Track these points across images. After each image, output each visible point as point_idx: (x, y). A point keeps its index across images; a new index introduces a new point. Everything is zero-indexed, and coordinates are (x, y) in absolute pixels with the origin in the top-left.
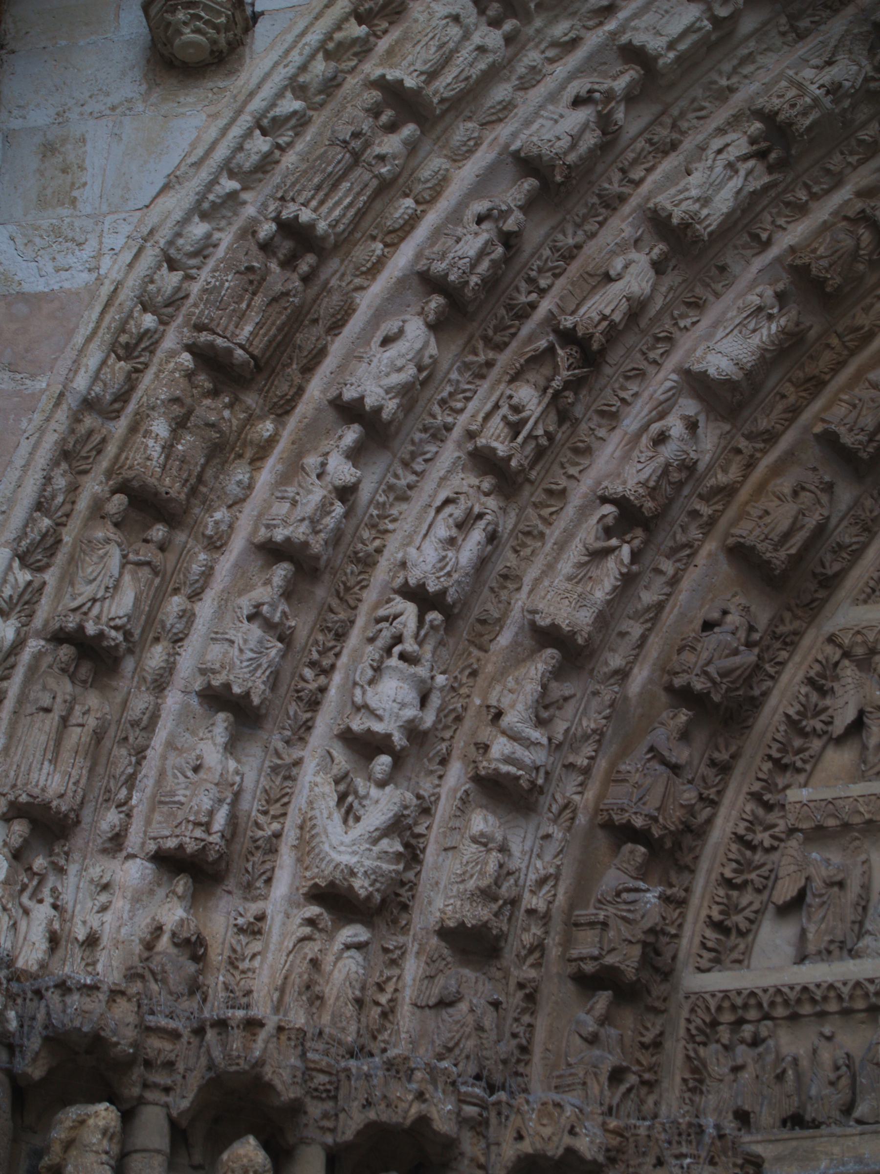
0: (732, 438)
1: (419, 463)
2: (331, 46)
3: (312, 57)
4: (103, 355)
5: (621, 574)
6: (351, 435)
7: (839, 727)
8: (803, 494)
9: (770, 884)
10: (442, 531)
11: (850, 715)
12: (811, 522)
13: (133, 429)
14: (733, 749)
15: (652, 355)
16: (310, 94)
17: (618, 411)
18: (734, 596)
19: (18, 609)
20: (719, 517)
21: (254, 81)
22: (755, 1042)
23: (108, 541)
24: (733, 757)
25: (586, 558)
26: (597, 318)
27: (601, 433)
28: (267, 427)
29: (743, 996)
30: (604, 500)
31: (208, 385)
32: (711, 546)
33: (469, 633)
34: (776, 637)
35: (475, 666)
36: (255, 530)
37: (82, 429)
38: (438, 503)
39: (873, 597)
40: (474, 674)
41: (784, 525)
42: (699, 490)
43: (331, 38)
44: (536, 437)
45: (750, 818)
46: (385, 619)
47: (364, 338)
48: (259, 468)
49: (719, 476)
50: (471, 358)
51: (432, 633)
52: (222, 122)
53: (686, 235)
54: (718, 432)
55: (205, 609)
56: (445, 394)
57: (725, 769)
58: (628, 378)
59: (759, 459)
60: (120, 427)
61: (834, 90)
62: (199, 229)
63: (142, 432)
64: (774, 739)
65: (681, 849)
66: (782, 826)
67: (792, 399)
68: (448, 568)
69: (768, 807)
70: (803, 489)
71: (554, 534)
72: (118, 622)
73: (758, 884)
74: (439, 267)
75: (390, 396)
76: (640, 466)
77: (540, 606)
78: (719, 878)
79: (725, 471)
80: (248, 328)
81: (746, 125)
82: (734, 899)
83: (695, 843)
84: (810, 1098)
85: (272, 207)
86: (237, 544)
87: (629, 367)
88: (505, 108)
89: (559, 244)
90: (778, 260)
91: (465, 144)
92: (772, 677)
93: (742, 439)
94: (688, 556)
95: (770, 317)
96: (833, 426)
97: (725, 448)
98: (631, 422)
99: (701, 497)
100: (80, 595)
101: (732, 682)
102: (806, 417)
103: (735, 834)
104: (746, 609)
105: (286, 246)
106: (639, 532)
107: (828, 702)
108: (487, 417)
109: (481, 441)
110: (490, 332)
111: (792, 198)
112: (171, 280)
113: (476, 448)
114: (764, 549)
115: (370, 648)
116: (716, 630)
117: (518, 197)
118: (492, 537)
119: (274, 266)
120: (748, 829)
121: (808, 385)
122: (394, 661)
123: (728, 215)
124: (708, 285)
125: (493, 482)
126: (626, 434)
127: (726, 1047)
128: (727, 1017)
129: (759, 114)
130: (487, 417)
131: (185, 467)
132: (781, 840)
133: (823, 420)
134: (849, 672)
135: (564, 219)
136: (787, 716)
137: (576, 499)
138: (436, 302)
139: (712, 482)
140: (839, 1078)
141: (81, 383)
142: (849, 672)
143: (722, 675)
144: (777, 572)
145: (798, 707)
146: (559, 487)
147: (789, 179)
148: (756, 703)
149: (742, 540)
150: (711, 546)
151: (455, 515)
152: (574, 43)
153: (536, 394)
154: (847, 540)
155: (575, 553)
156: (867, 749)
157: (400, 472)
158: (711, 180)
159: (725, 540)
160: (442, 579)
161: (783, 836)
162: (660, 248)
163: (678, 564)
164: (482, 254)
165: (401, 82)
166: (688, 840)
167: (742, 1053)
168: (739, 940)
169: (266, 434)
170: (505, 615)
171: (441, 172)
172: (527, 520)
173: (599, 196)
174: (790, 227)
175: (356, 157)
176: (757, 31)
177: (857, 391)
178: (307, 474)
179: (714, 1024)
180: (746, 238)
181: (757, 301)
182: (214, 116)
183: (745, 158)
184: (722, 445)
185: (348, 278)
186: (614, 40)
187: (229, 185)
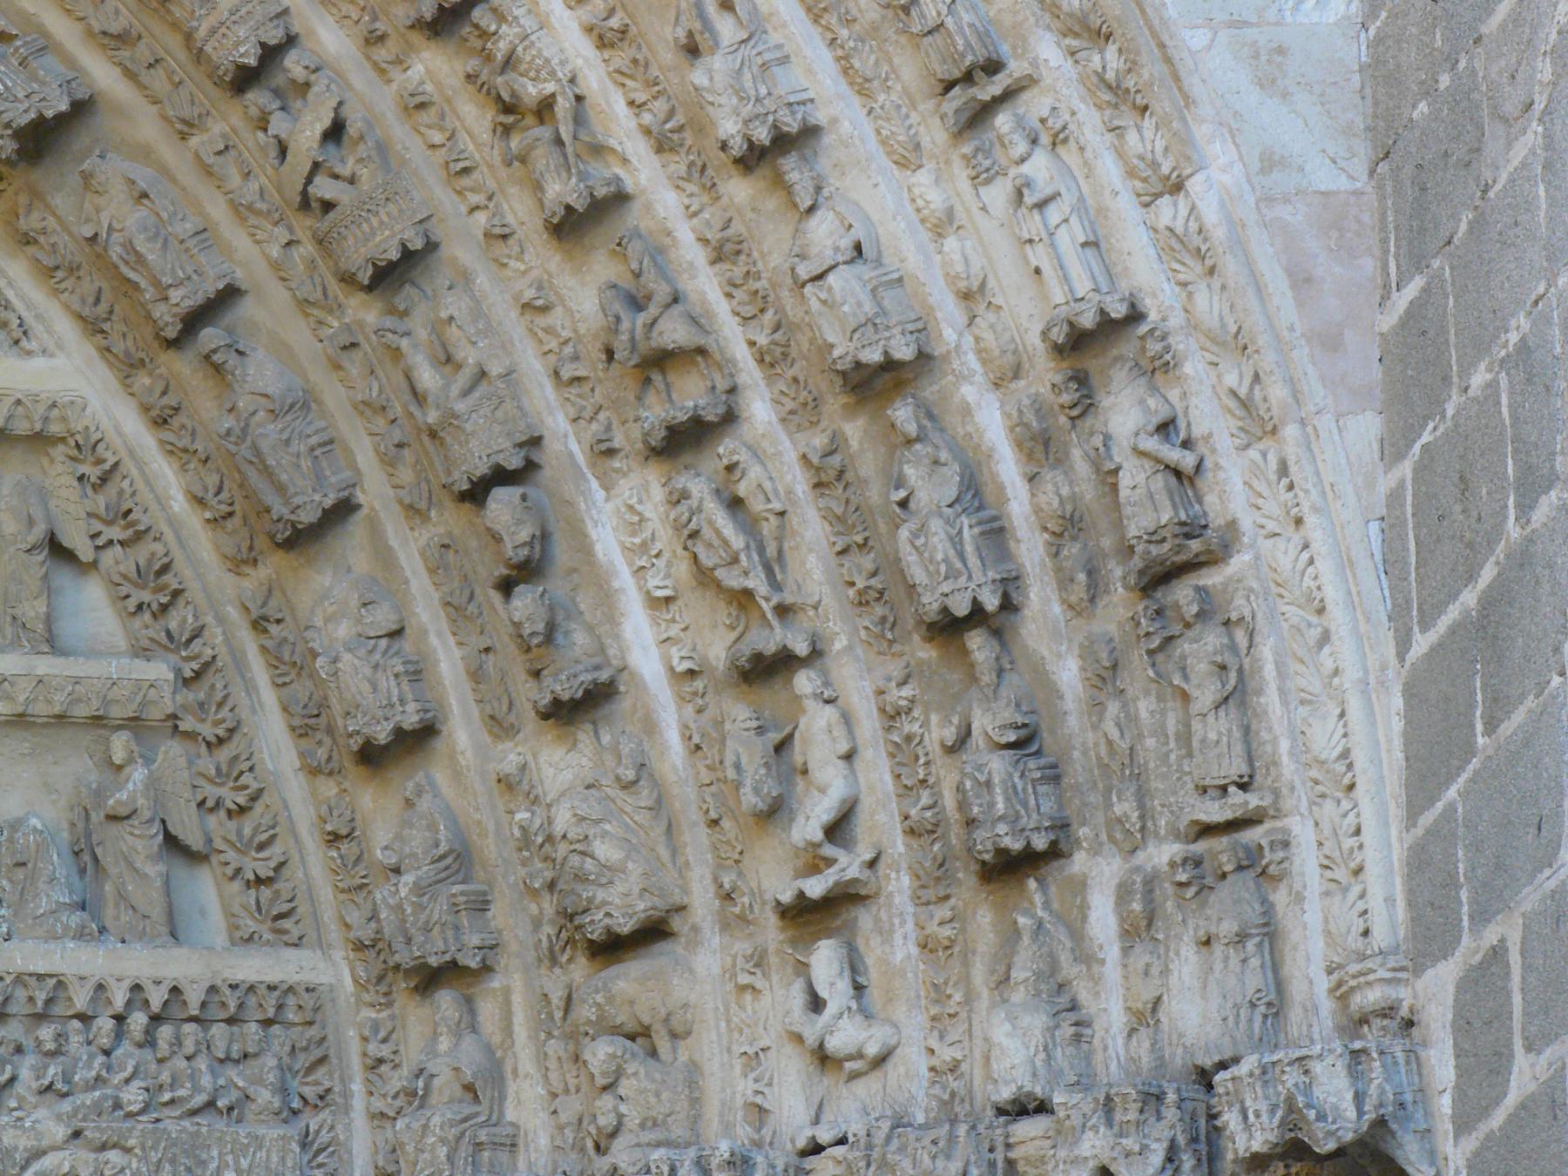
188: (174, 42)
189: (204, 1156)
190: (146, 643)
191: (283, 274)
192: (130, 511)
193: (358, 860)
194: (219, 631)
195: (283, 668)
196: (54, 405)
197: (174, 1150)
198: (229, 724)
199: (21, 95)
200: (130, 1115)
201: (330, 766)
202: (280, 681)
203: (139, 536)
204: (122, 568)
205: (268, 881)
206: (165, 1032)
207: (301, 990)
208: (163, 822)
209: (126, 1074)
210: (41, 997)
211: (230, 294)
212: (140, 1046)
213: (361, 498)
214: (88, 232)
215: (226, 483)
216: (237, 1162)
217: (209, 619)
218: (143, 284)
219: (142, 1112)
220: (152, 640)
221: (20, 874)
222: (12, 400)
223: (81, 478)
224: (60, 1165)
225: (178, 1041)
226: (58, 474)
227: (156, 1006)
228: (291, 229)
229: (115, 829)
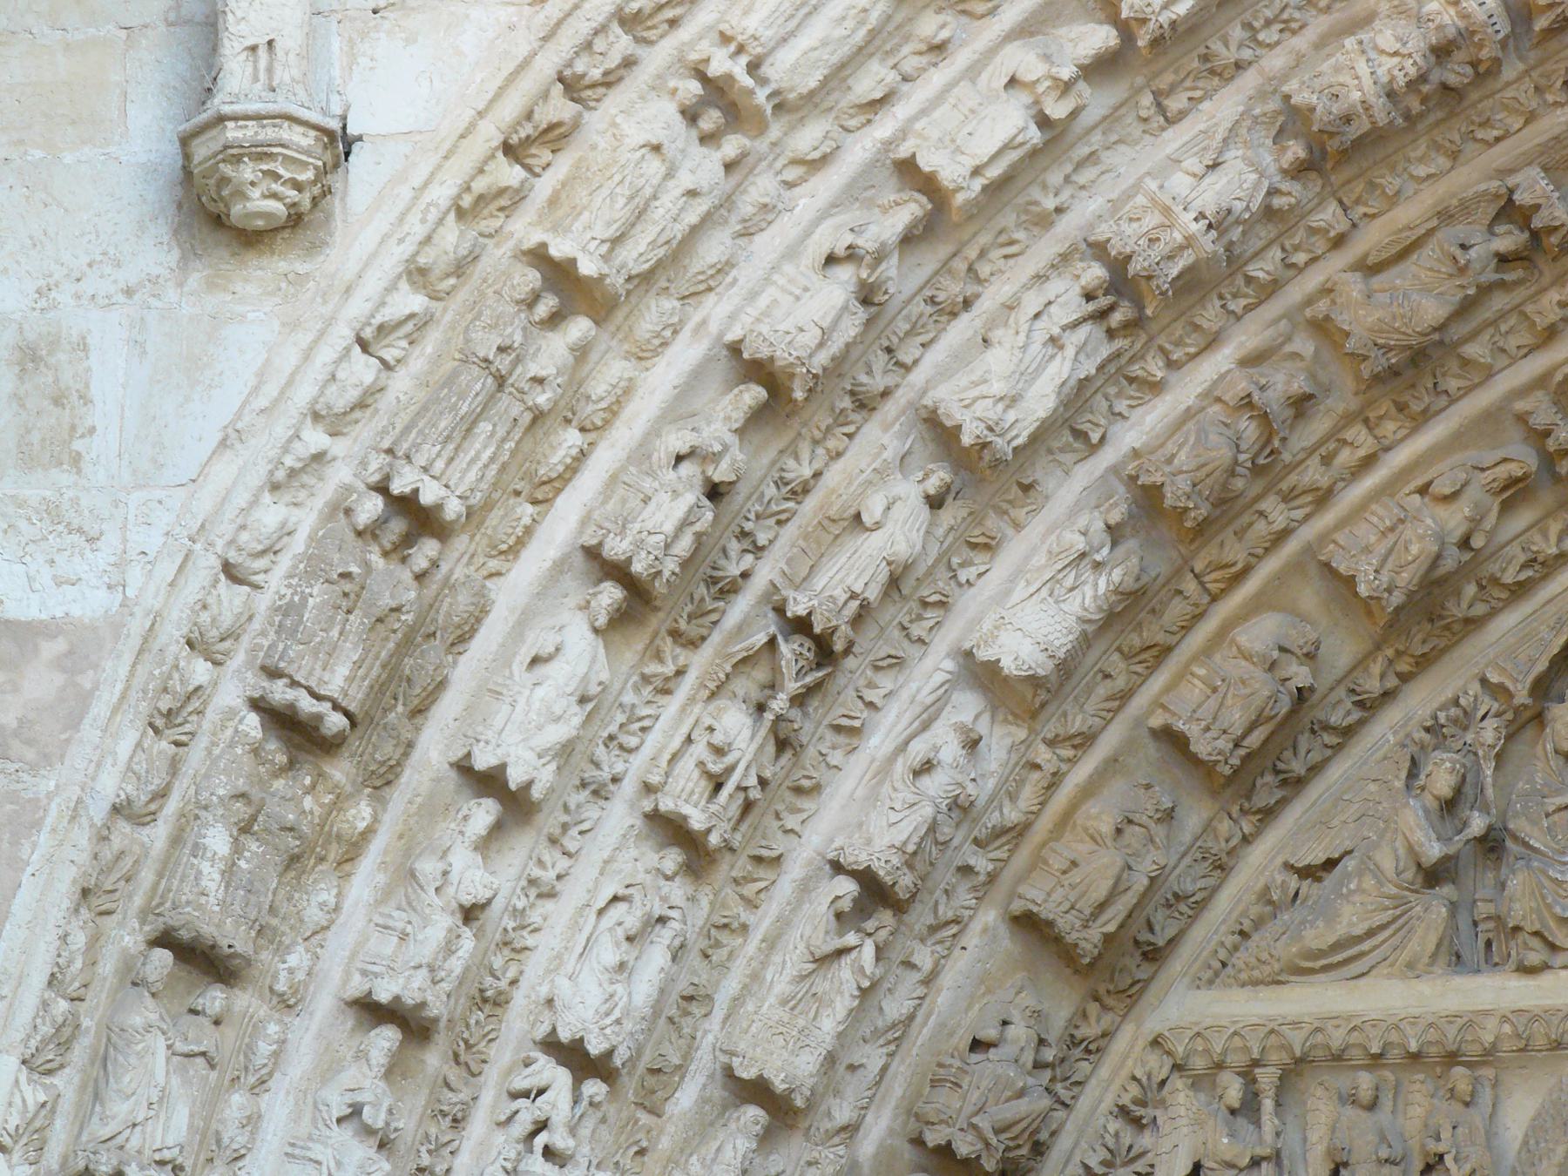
1: (573, 838)
2: (467, 201)
3: (441, 221)
4: (138, 735)
5: (859, 988)
6: (484, 813)
8: (1130, 830)
10: (608, 953)
13: (176, 840)
15: (917, 630)
16: (433, 277)
19: (24, 1140)
21: (352, 267)
23: (148, 1028)
25: (812, 966)
26: (845, 596)
27: (836, 758)
28: (360, 813)
30: (837, 867)
31: (282, 759)
33: (636, 1094)
34: (1074, 1042)
35: (644, 1144)
36: (346, 981)
37: (107, 854)
38: (601, 904)
40: (641, 1152)
41: (1100, 891)
42: (976, 833)
43: (468, 189)
44: (746, 789)
46: (525, 1094)
47: (503, 659)
48: (349, 875)
49: (1006, 811)
50: (652, 668)
51: (591, 1111)
52: (304, 339)
53: (981, 458)
54: (1008, 741)
55: (278, 1107)
56: (613, 728)
58: (877, 668)
60: (157, 835)
61: (1218, 224)
62: (271, 515)
63: (189, 845)
68: (617, 1014)
70: (1130, 822)
71: (762, 922)
72: (167, 1155)
74: (616, 548)
75: (543, 761)
76: (894, 817)
77: (742, 1047)
79: (1013, 797)
80: (343, 670)
81: (1080, 265)
85: (377, 462)
86: (324, 1003)
87: (883, 654)
88: (719, 271)
89: (788, 476)
90: (1114, 470)
91: (658, 335)
93: (1042, 748)
94: (954, 936)
95: (1098, 566)
96: (1180, 724)
97: (1017, 764)
98: (878, 742)
99: (976, 842)
100: (113, 1118)
101: (1012, 1139)
104: (1037, 1014)
105: (397, 526)
107: (1146, 1140)
108: (674, 758)
109: (666, 804)
110: (683, 625)
111: (1140, 373)
112: (232, 598)
113: (656, 810)
115: (500, 1138)
116: (992, 1052)
117: (734, 415)
118: (678, 953)
119: (376, 558)
122: (536, 1163)
123: (1044, 421)
124: (1006, 512)
125: (680, 859)
129: (1099, 250)
130: (674, 758)
131: (253, 899)
134: (1181, 1098)
135: (800, 434)
137: (794, 871)
138: (610, 594)
139: (993, 819)
141: (109, 786)
142: (1181, 1097)
143: (997, 1132)
145: (1103, 1154)
146: (774, 854)
147: (1138, 346)
149: (1035, 909)
150: (989, 916)
151: (628, 925)
152: (825, 160)
153: (749, 721)
154: (1189, 887)
155: (791, 959)
157: (546, 858)
158: (1022, 368)
159: (1009, 904)
160: (608, 1031)
162: (939, 477)
164: (685, 523)
165: (573, 261)
169: (362, 826)
170: (687, 1056)
171: (623, 384)
172: (724, 906)
173: (852, 393)
174: (1135, 415)
175: (501, 381)
176: (1105, 118)
178: (422, 888)
180: (1067, 437)
181: (1080, 544)
182: (292, 325)
183: (1075, 325)
184: (1012, 762)
185: (480, 560)
186: (887, 151)
187: (316, 438)
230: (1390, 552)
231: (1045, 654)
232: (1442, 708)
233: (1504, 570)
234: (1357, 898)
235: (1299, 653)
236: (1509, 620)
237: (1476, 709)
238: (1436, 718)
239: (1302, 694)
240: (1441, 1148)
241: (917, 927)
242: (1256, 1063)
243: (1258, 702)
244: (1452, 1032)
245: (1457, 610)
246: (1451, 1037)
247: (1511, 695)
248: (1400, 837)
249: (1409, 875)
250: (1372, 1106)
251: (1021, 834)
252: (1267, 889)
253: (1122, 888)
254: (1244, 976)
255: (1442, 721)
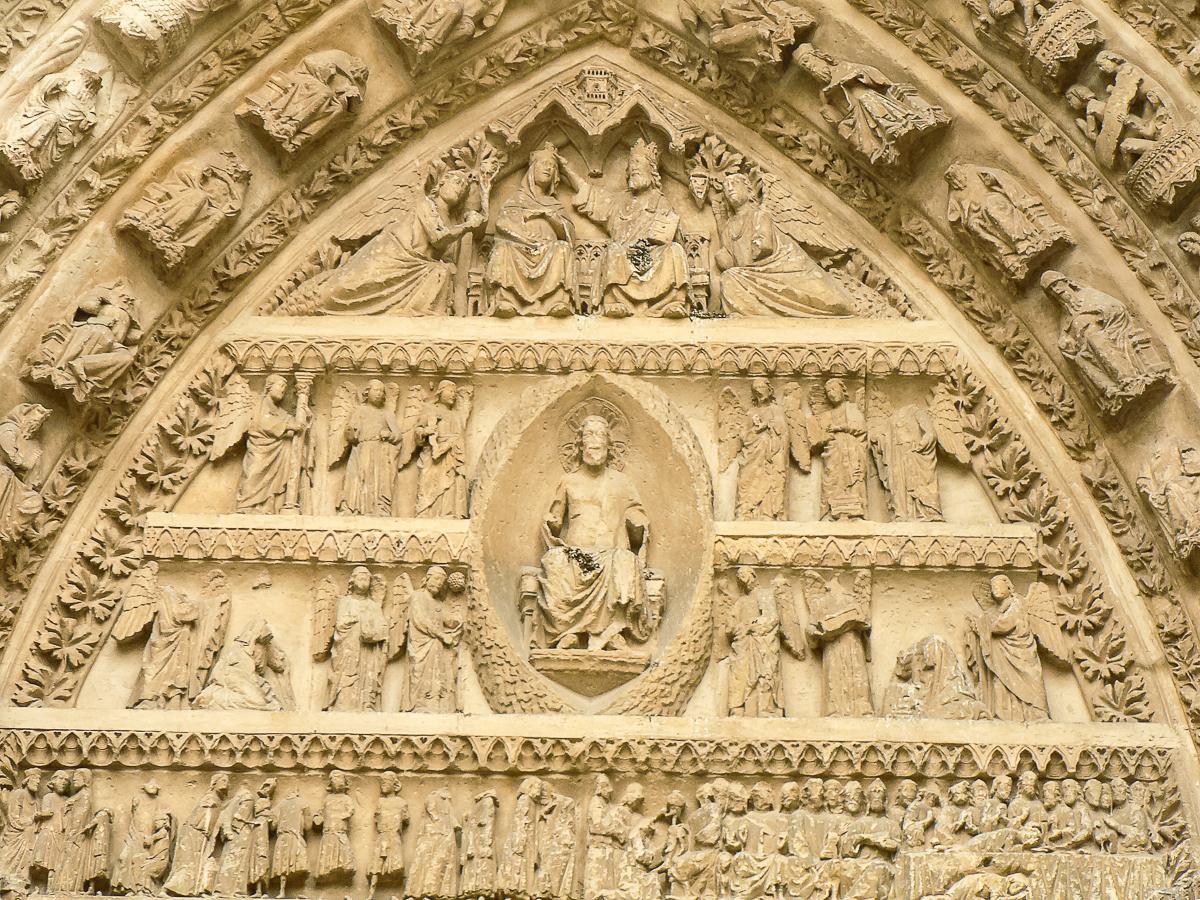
0: (141, 105)
7: (218, 450)
8: (213, 181)
9: (114, 615)
11: (234, 438)
12: (218, 214)
14: (93, 458)
17: (8, 54)
18: (118, 285)
20: (113, 193)
22: (67, 792)
24: (90, 467)
29: (61, 737)
32: (100, 225)
34: (161, 339)
39: (279, 308)
41: (185, 214)
45: (102, 539)
54: (124, 96)
57: (80, 479)
58: (26, 18)
59: (170, 134)
64: (143, 454)
65: (15, 563)
66: (137, 552)
67: (215, 72)
69: (125, 529)
70: (214, 175)
73: (101, 612)
78: (56, 602)
82: (69, 627)
83: (32, 559)
84: (120, 861)
87: (29, 6)
92: (150, 383)
93: (152, 108)
97: (130, 115)
99: (93, 166)
101: (99, 382)
102: (230, 94)
103: (81, 554)
104: (130, 302)
106: (14, 196)
107: (211, 419)
114: (158, 237)
116: (91, 320)
120: (97, 550)
121: (237, 58)
126: (14, 82)
127: (33, 794)
128: (40, 759)
132: (134, 568)
133: (248, 101)
134: (238, 389)
136: (162, 429)
139: (109, 152)
140: (156, 841)
142: (238, 385)
144: (170, 265)
148: (126, 410)
149: (135, 223)
150: (100, 225)
154: (259, 241)
156: (246, 477)
161: (137, 563)
163: (57, 240)
166: (25, 554)
167: (50, 802)
168: (69, 674)
177: (292, 73)
179: (24, 766)
184: (126, 112)
188: (1011, 68)
189: (1089, 877)
190: (1014, 517)
191: (1102, 224)
192: (995, 421)
193: (1191, 653)
194: (1068, 501)
195: (1122, 521)
196: (934, 353)
197: (1064, 872)
198: (1083, 565)
199: (900, 116)
200: (1028, 848)
201: (1163, 586)
202: (1118, 531)
203: (1005, 439)
204: (991, 464)
205: (1121, 677)
206: (1051, 787)
207: (1154, 752)
208: (1036, 638)
209: (1023, 817)
210: (951, 762)
211: (1060, 250)
212: (1031, 797)
213: (1173, 379)
214: (953, 217)
215: (1067, 390)
216: (1116, 881)
217: (1060, 493)
218: (998, 243)
219: (1037, 845)
220: (1017, 513)
221: (929, 675)
222: (904, 349)
223: (957, 405)
224: (975, 885)
225: (1061, 794)
226: (942, 399)
227: (1042, 766)
228: (1107, 189)
229: (998, 645)
230: (424, 12)
231: (155, 25)
232: (456, 146)
233: (507, 53)
234: (381, 258)
235: (352, 77)
236: (507, 96)
237: (481, 151)
238: (451, 152)
239: (352, 104)
240: (427, 430)
241: (41, 218)
242: (297, 368)
243: (317, 99)
244: (442, 354)
245: (471, 76)
246: (441, 357)
247: (504, 138)
248: (417, 222)
249: (421, 249)
250: (380, 404)
251: (129, 170)
252: (318, 253)
253: (202, 215)
254: (293, 308)
255: (456, 153)
